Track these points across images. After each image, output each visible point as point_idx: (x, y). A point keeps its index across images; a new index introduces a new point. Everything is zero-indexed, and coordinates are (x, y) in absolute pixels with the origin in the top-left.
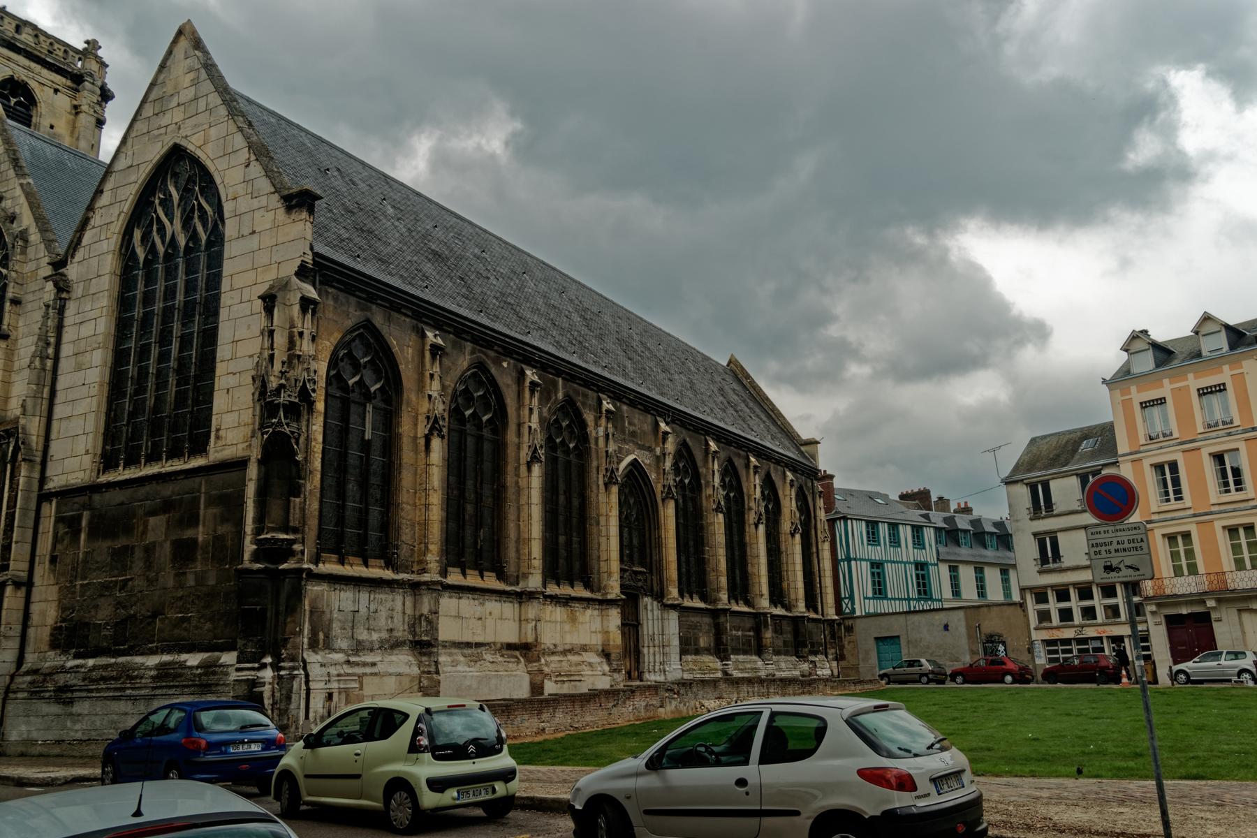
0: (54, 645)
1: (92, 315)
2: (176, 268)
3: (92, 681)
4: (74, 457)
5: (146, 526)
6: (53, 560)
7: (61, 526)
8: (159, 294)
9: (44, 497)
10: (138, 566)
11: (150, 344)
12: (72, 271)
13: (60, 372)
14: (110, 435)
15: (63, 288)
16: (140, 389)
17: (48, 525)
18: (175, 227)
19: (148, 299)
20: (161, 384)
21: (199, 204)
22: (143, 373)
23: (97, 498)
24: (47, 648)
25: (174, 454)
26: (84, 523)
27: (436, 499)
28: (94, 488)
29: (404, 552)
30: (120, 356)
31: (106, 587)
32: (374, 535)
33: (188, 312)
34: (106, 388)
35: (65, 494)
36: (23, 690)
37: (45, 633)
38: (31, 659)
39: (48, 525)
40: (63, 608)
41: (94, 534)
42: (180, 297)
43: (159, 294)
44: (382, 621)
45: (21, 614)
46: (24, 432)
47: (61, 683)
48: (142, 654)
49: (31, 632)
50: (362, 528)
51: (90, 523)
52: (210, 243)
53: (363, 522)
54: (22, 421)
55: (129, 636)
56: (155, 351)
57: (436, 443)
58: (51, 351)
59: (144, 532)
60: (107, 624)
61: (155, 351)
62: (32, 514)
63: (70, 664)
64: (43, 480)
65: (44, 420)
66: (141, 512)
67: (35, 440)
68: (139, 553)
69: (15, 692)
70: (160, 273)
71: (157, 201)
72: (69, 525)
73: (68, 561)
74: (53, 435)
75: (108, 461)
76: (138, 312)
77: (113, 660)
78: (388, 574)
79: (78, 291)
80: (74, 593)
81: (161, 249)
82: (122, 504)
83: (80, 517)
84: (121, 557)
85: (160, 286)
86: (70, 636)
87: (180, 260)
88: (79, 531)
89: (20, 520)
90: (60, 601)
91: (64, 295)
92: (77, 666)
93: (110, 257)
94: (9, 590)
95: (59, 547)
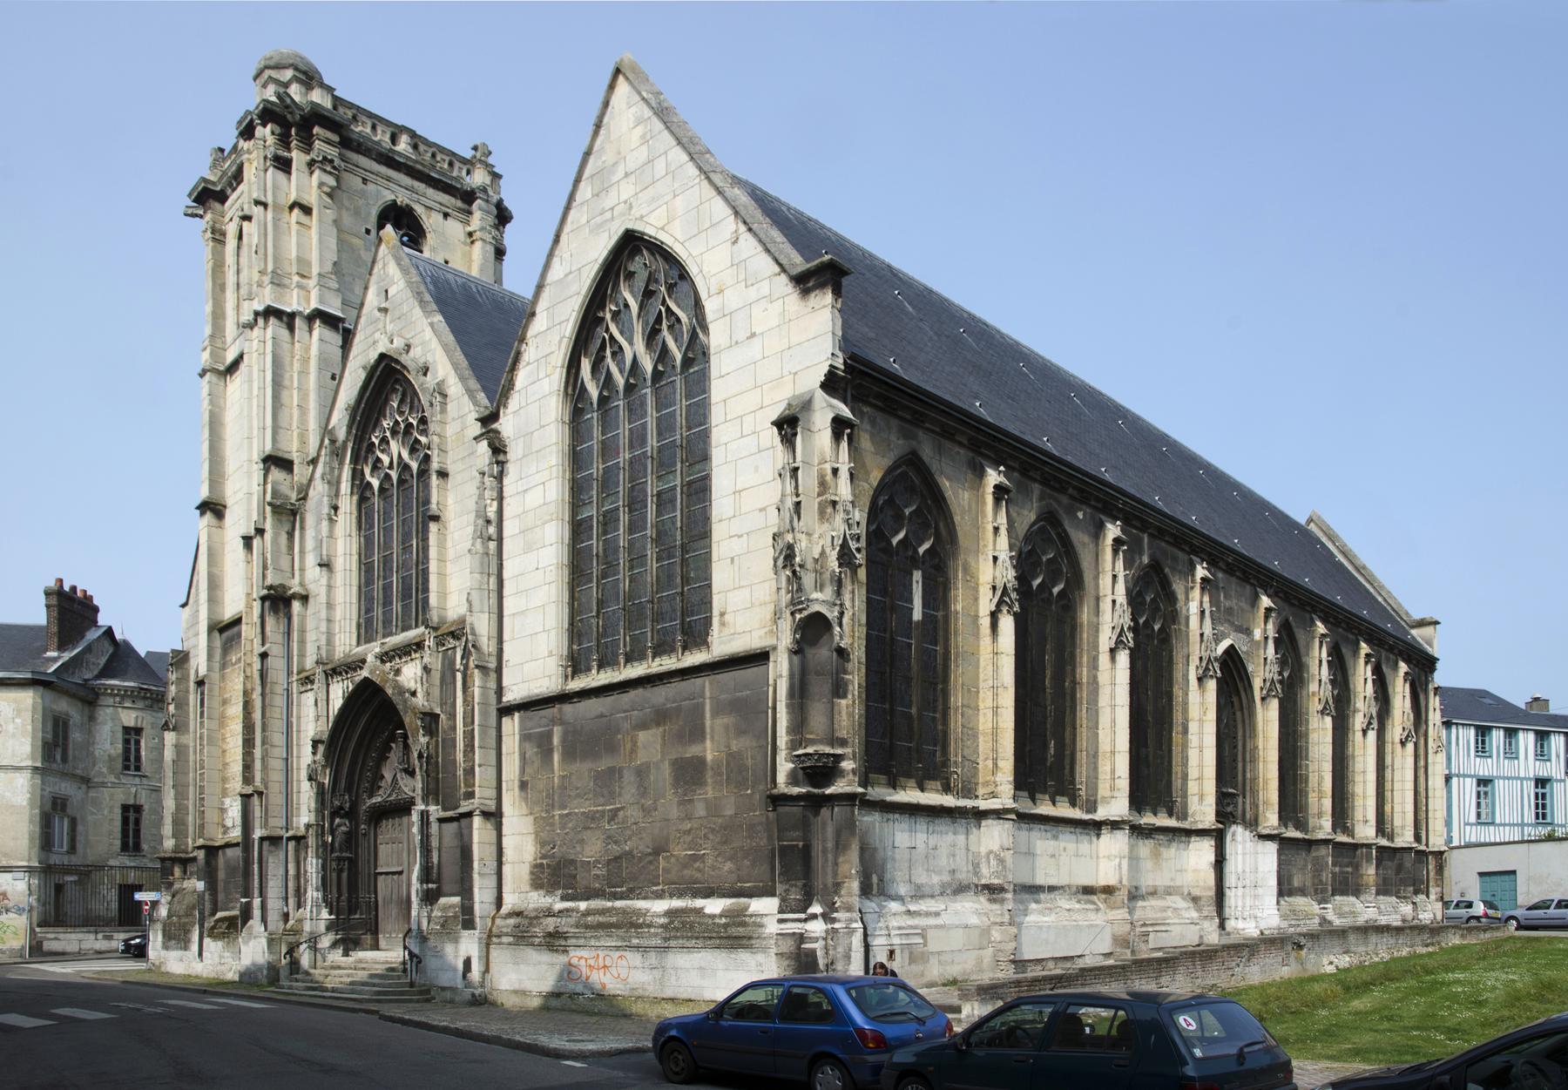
0: (537, 884)
1: (538, 478)
2: (643, 404)
3: (587, 927)
4: (534, 659)
5: (634, 743)
6: (523, 785)
7: (527, 745)
8: (623, 441)
9: (506, 711)
10: (629, 793)
11: (617, 509)
12: (506, 425)
13: (505, 556)
14: (575, 631)
15: (498, 449)
16: (609, 567)
17: (511, 744)
18: (636, 347)
19: (608, 449)
20: (637, 560)
21: (668, 309)
22: (610, 548)
23: (567, 708)
24: (528, 888)
25: (661, 649)
26: (556, 740)
28: (563, 698)
30: (578, 529)
31: (592, 817)
33: (664, 465)
34: (566, 572)
36: (507, 935)
37: (525, 871)
38: (510, 901)
39: (511, 744)
40: (542, 843)
41: (570, 754)
42: (652, 442)
43: (623, 441)
44: (943, 861)
45: (494, 848)
46: (474, 634)
47: (551, 929)
48: (645, 898)
49: (506, 869)
51: (564, 741)
52: (687, 362)
54: (469, 620)
55: (626, 875)
56: (624, 518)
58: (492, 530)
59: (633, 751)
60: (597, 861)
61: (624, 518)
62: (493, 733)
63: (559, 906)
64: (500, 691)
65: (494, 617)
66: (627, 726)
67: (487, 645)
68: (629, 777)
69: (499, 937)
70: (622, 413)
71: (608, 316)
72: (539, 743)
73: (541, 785)
74: (506, 637)
75: (576, 664)
76: (596, 468)
77: (609, 904)
80: (552, 825)
81: (620, 381)
82: (602, 716)
83: (549, 735)
84: (607, 781)
85: (623, 430)
86: (554, 873)
87: (648, 390)
88: (551, 751)
89: (481, 739)
90: (537, 834)
91: (501, 458)
92: (567, 910)
93: (554, 399)
94: (477, 821)
95: (528, 770)
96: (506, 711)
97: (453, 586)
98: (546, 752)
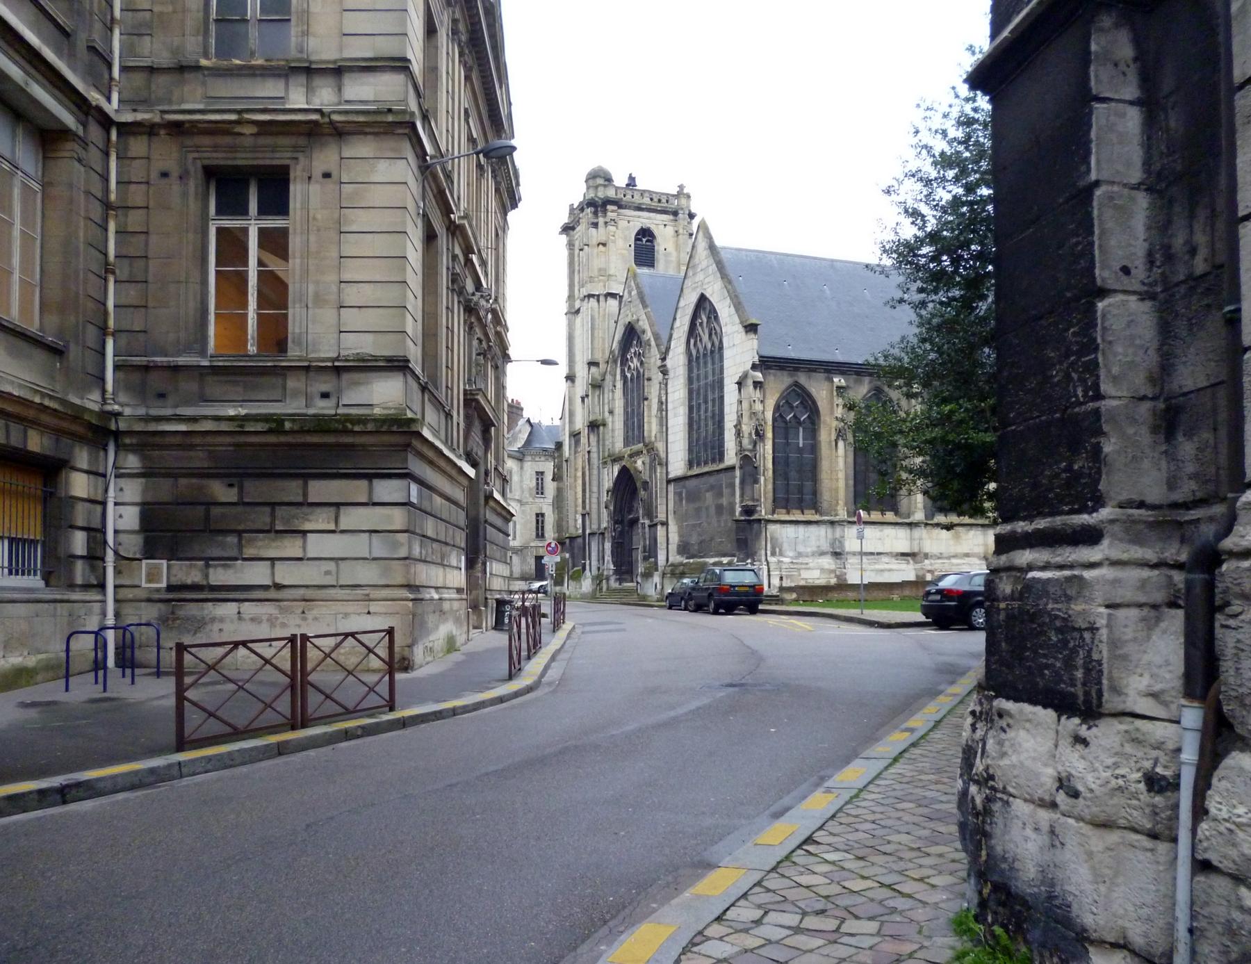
9: (669, 482)
10: (703, 514)
17: (671, 496)
18: (705, 338)
27: (841, 475)
29: (825, 505)
30: (691, 408)
31: (694, 526)
32: (807, 497)
35: (677, 480)
39: (671, 496)
41: (688, 500)
50: (799, 491)
53: (801, 491)
57: (841, 444)
72: (678, 494)
75: (690, 464)
78: (817, 518)
79: (671, 374)
84: (698, 510)
96: (669, 482)
97: (652, 428)
98: (681, 500)
